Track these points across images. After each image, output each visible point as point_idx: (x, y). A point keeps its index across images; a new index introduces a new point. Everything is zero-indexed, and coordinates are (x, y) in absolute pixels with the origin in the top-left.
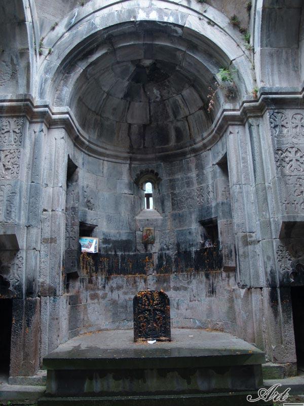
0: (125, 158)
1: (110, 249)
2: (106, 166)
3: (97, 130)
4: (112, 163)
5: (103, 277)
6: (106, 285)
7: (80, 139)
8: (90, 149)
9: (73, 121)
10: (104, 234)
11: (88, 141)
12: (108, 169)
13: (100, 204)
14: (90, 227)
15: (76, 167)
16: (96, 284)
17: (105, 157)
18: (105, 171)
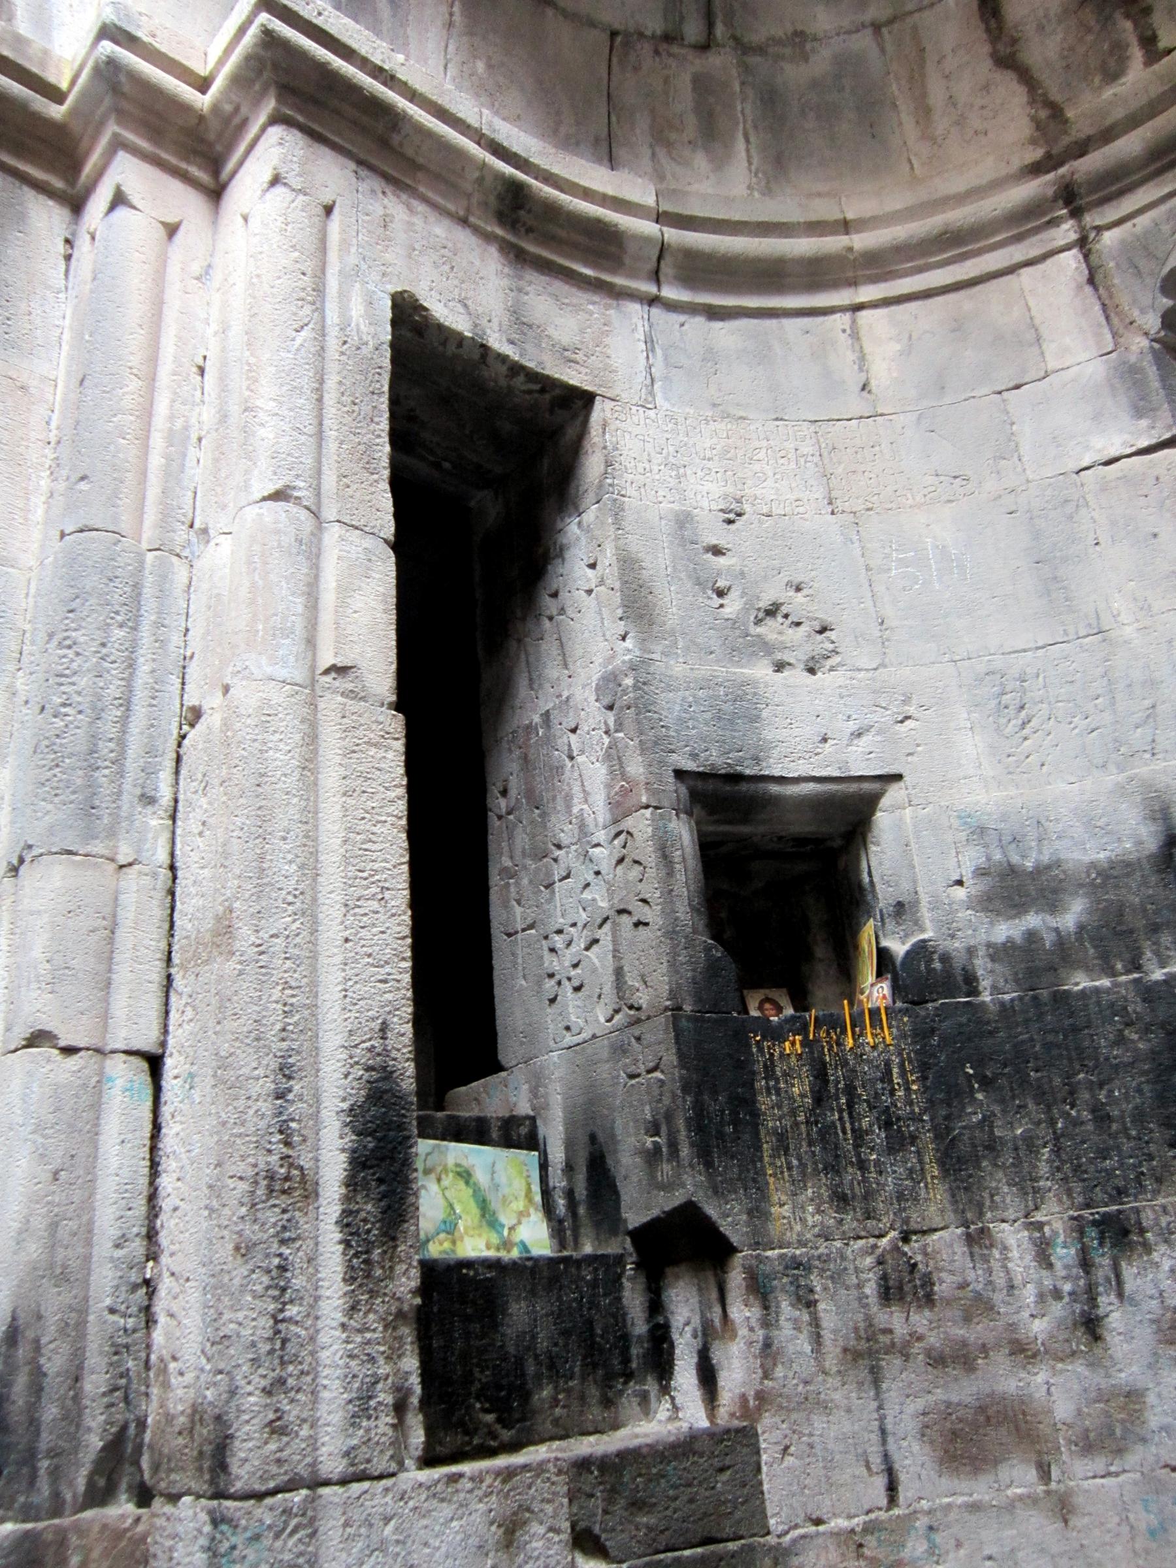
0: (1027, 220)
1: (1065, 953)
2: (887, 339)
3: (741, 145)
4: (939, 300)
5: (1055, 1216)
6: (1106, 1301)
7: (552, 211)
8: (702, 270)
9: (346, 53)
10: (982, 830)
11: (660, 217)
12: (907, 352)
13: (888, 611)
14: (823, 806)
15: (588, 399)
16: (978, 1306)
17: (853, 283)
18: (882, 371)
